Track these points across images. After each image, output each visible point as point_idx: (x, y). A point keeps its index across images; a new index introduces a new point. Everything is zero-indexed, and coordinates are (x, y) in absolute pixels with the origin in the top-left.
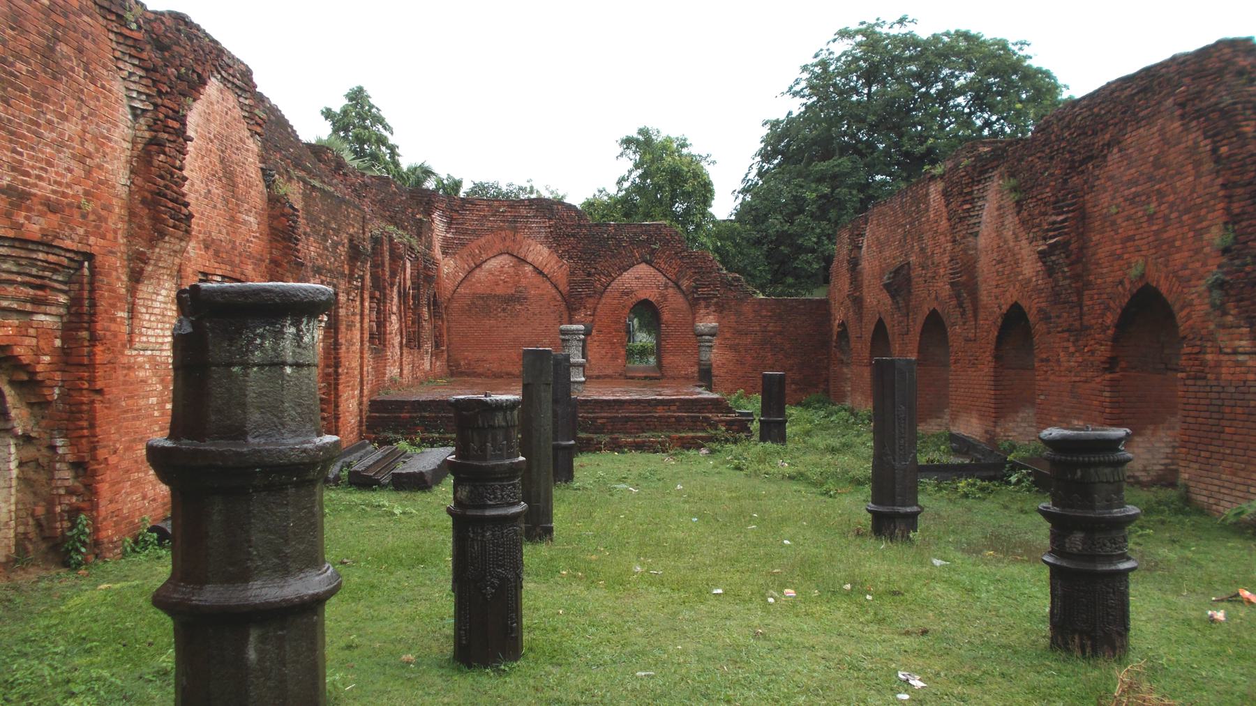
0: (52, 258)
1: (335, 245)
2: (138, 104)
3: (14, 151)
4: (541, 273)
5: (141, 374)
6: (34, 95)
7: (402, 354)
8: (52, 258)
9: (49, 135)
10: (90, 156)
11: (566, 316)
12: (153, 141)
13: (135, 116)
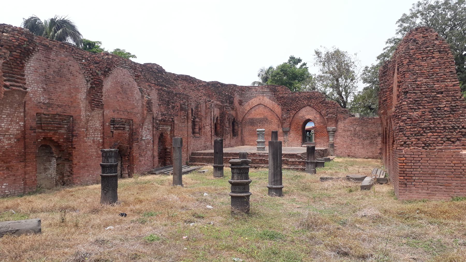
0: (60, 117)
1: (173, 107)
2: (88, 79)
3: (49, 95)
4: (272, 110)
5: (90, 144)
6: (54, 82)
8: (60, 117)
10: (72, 93)
12: (91, 87)
13: (88, 82)
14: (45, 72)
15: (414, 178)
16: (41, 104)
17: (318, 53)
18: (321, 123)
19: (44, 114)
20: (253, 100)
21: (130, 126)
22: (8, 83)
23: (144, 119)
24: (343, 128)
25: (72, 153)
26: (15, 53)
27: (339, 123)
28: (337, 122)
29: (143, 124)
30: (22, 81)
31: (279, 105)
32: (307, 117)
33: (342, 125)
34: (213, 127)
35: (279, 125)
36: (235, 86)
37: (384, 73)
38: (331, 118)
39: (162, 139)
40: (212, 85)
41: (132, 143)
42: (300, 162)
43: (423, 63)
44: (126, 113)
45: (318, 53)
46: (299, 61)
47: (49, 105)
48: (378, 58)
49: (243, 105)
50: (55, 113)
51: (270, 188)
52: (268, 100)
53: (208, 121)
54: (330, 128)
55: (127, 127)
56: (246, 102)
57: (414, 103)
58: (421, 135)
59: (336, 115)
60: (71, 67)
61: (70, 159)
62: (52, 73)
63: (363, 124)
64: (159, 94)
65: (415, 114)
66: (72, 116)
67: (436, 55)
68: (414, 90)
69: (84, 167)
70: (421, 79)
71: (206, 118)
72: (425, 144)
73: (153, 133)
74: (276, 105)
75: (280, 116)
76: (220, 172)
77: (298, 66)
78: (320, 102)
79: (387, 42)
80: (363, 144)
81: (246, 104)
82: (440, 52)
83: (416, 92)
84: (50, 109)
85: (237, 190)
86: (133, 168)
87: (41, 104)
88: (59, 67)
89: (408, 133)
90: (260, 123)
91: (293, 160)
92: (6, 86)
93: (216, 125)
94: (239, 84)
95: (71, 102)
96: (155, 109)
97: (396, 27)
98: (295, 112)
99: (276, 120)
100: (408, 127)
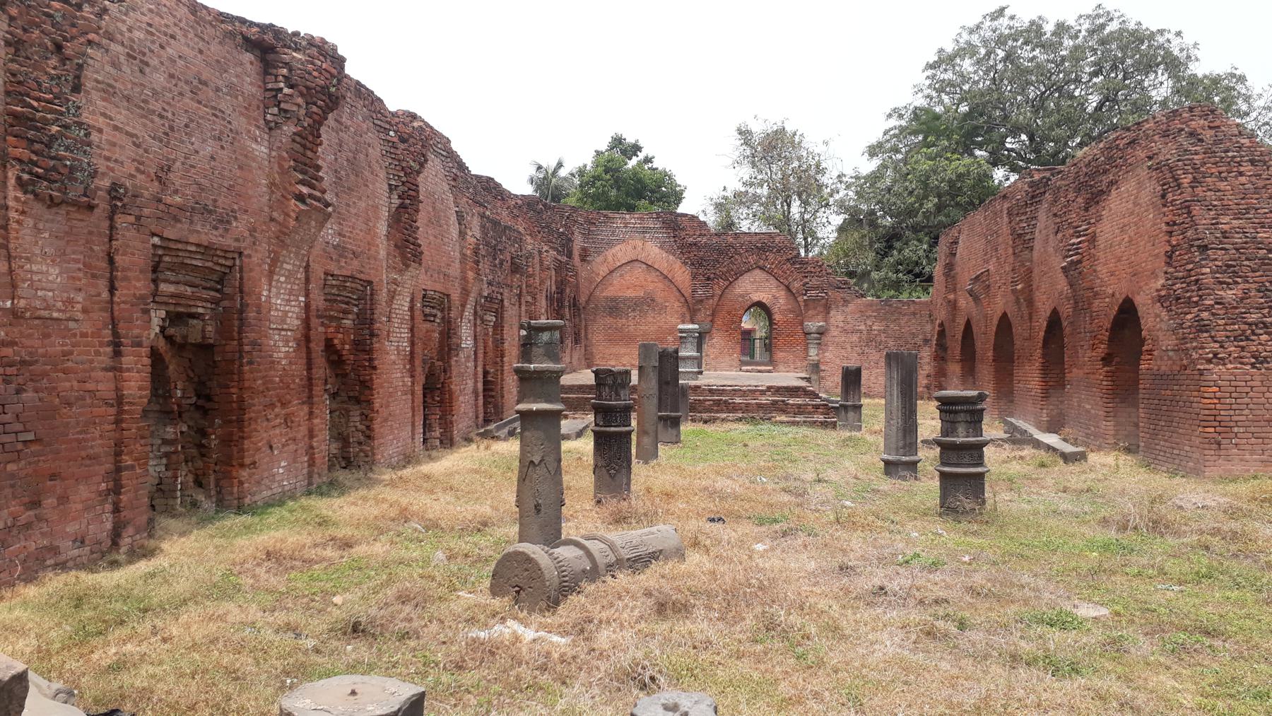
1: (501, 264)
4: (666, 277)
9: (353, 211)
11: (688, 317)
12: (402, 206)
13: (391, 189)
15: (1236, 430)
16: (330, 249)
17: (745, 134)
18: (791, 311)
20: (618, 248)
21: (442, 311)
22: (305, 190)
23: (465, 293)
24: (841, 324)
25: (371, 379)
26: (315, 109)
27: (832, 313)
28: (827, 309)
31: (685, 263)
32: (756, 297)
33: (840, 318)
35: (683, 315)
37: (1033, 197)
38: (816, 300)
40: (529, 204)
41: (449, 358)
42: (817, 407)
43: (1222, 185)
45: (745, 134)
46: (636, 149)
48: (873, 151)
49: (589, 262)
50: (349, 274)
51: (887, 463)
52: (657, 250)
54: (812, 325)
55: (439, 314)
56: (599, 253)
57: (1225, 272)
58: (1247, 339)
60: (370, 150)
61: (363, 398)
63: (888, 316)
64: (483, 227)
65: (1229, 295)
66: (370, 283)
67: (1247, 168)
68: (1221, 243)
69: (386, 420)
70: (1225, 219)
72: (1256, 358)
73: (475, 332)
74: (678, 264)
76: (674, 432)
77: (632, 163)
79: (890, 116)
81: (600, 259)
82: (1252, 162)
83: (1227, 246)
85: (966, 460)
86: (451, 423)
87: (330, 249)
89: (1221, 336)
90: (634, 310)
91: (799, 401)
92: (300, 198)
97: (921, 78)
98: (727, 283)
99: (677, 304)
100: (1220, 322)
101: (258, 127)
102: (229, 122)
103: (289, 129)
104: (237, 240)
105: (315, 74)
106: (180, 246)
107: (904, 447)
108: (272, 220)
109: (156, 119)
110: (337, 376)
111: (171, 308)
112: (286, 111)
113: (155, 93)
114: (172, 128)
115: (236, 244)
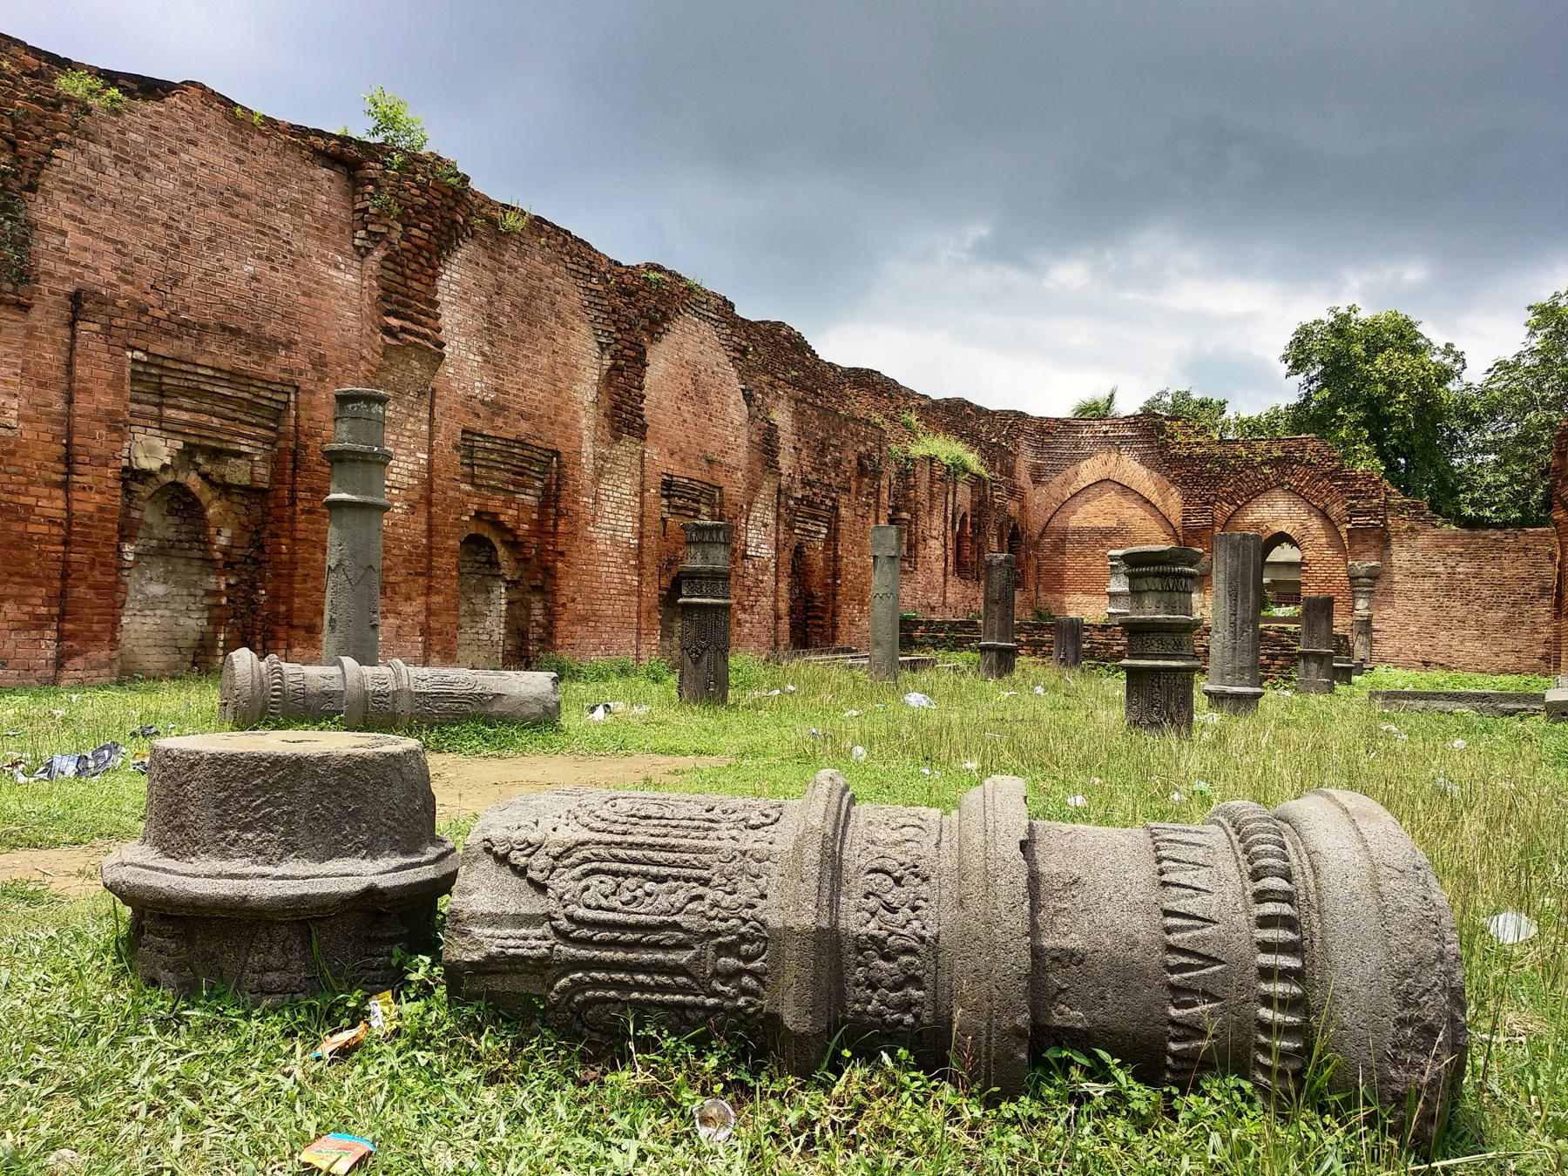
5: (602, 547)
7: (945, 582)
12: (614, 367)
13: (603, 349)
14: (491, 303)
19: (482, 435)
26: (415, 232)
29: (750, 504)
30: (431, 321)
34: (950, 542)
36: (1021, 415)
39: (798, 566)
44: (703, 463)
47: (497, 408)
49: (1044, 484)
50: (513, 437)
53: (937, 522)
59: (1383, 521)
61: (547, 588)
62: (508, 309)
63: (1482, 552)
66: (557, 454)
71: (930, 513)
73: (777, 540)
75: (1176, 517)
78: (1325, 474)
80: (1481, 624)
84: (499, 422)
88: (526, 292)
92: (388, 330)
93: (959, 538)
94: (1036, 409)
95: (557, 407)
96: (785, 461)
98: (1233, 508)
101: (341, 254)
102: (288, 243)
103: (378, 254)
104: (284, 371)
105: (413, 191)
106: (184, 367)
107: (1232, 673)
108: (362, 358)
109: (159, 229)
110: (518, 561)
111: (194, 440)
112: (375, 234)
113: (158, 199)
114: (186, 241)
115: (285, 376)
